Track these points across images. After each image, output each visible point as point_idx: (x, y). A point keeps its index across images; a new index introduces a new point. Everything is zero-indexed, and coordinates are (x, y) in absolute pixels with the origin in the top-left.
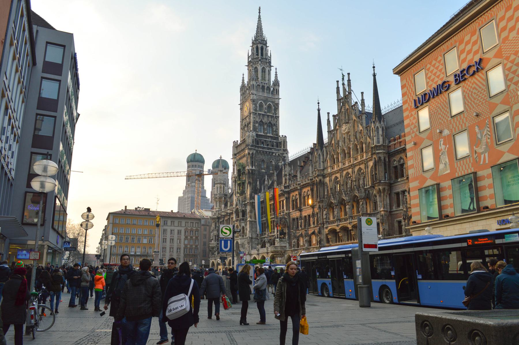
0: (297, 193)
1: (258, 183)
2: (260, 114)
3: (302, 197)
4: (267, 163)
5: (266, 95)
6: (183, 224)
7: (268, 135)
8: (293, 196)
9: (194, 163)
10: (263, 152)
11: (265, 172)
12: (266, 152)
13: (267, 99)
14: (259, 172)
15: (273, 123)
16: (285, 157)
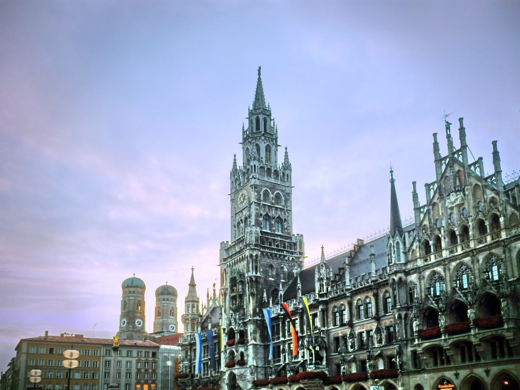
0: (344, 302)
1: (265, 295)
2: (266, 205)
3: (354, 307)
4: (277, 269)
5: (273, 181)
6: (135, 353)
7: (276, 233)
8: (335, 307)
9: (132, 289)
10: (271, 254)
11: (274, 281)
12: (276, 255)
13: (275, 186)
14: (266, 281)
15: (283, 217)
16: (301, 262)
